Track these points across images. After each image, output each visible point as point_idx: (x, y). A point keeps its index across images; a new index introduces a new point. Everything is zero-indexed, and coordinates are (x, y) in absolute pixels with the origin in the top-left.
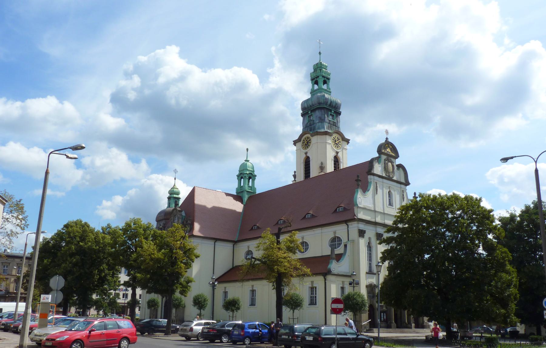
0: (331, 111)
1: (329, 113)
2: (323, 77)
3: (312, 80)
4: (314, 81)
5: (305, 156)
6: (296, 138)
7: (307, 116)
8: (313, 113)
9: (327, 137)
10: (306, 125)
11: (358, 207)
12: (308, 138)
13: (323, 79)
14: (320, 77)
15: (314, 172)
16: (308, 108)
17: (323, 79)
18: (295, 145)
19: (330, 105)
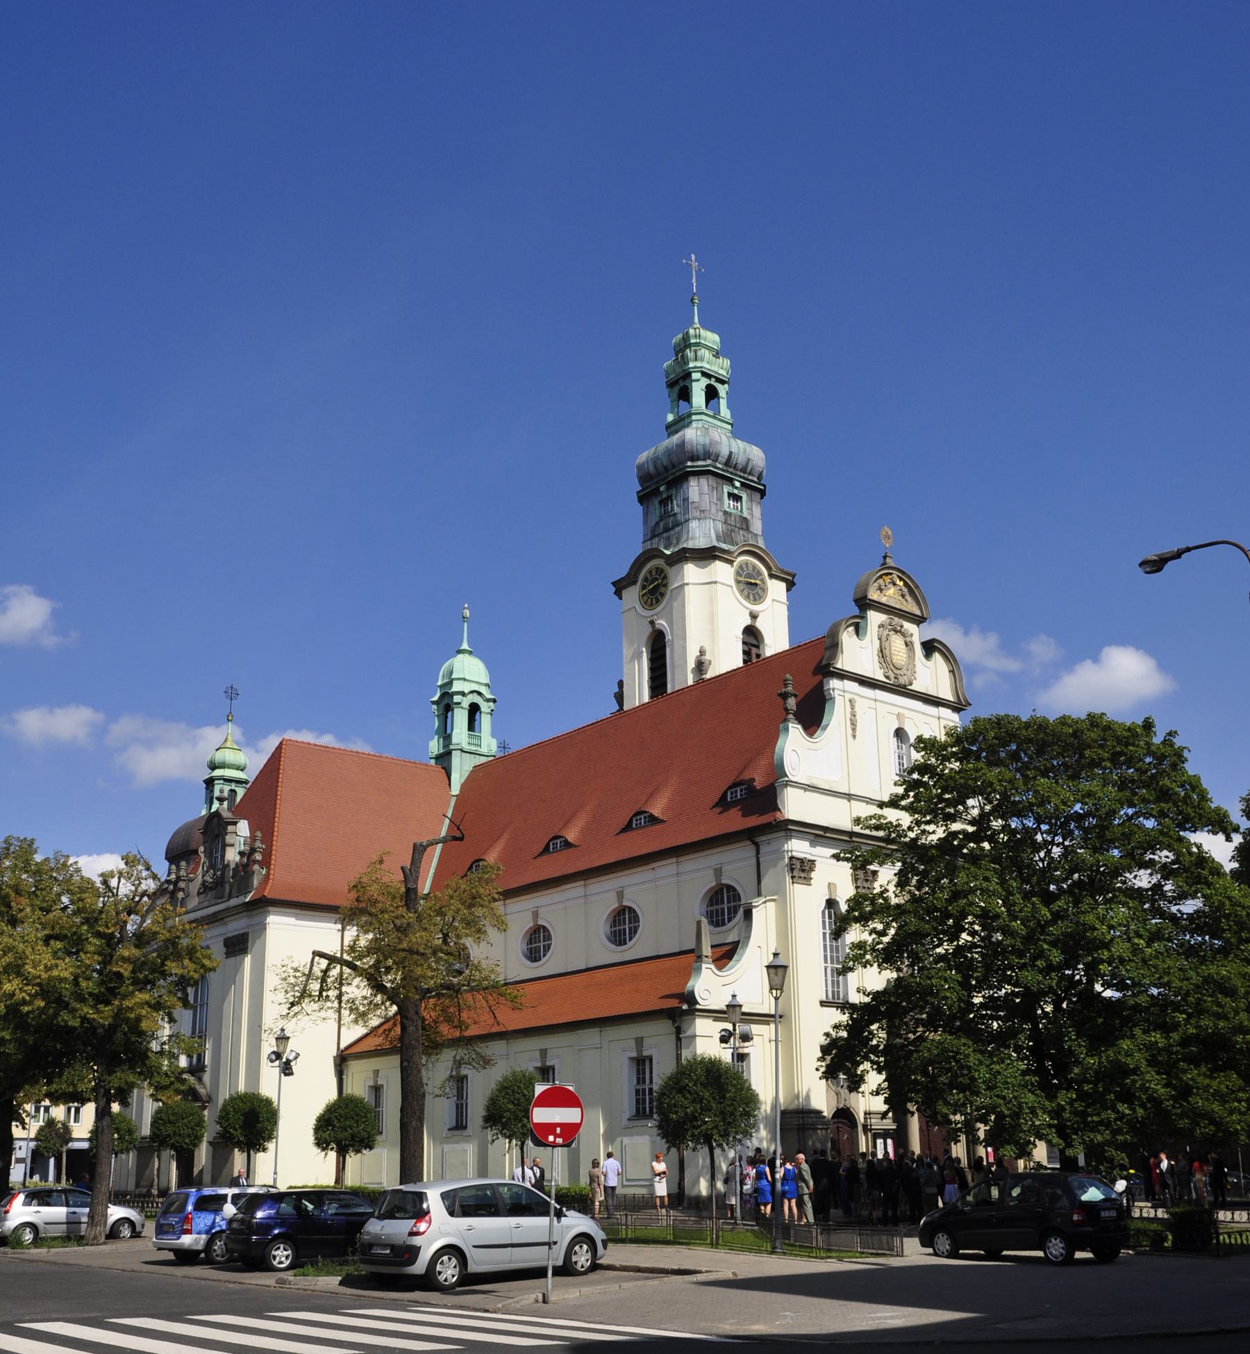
0: (730, 481)
1: (727, 489)
2: (705, 374)
3: (671, 385)
4: (677, 388)
5: (650, 629)
6: (623, 572)
7: (656, 502)
8: (673, 492)
9: (718, 565)
10: (653, 530)
11: (789, 783)
12: (660, 571)
13: (705, 382)
14: (695, 376)
15: (682, 677)
16: (658, 474)
17: (705, 382)
18: (618, 593)
19: (728, 463)
